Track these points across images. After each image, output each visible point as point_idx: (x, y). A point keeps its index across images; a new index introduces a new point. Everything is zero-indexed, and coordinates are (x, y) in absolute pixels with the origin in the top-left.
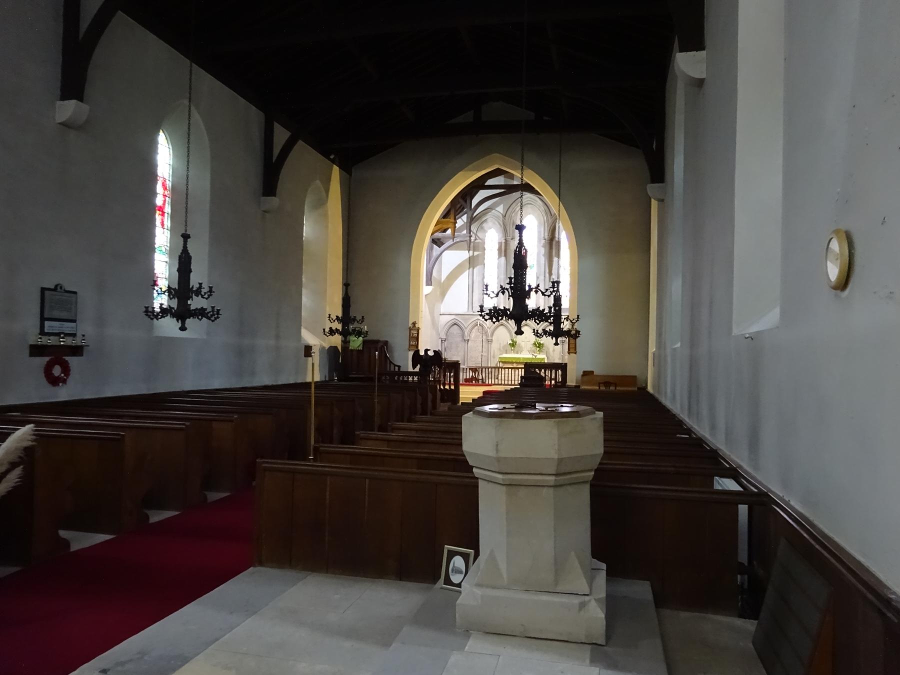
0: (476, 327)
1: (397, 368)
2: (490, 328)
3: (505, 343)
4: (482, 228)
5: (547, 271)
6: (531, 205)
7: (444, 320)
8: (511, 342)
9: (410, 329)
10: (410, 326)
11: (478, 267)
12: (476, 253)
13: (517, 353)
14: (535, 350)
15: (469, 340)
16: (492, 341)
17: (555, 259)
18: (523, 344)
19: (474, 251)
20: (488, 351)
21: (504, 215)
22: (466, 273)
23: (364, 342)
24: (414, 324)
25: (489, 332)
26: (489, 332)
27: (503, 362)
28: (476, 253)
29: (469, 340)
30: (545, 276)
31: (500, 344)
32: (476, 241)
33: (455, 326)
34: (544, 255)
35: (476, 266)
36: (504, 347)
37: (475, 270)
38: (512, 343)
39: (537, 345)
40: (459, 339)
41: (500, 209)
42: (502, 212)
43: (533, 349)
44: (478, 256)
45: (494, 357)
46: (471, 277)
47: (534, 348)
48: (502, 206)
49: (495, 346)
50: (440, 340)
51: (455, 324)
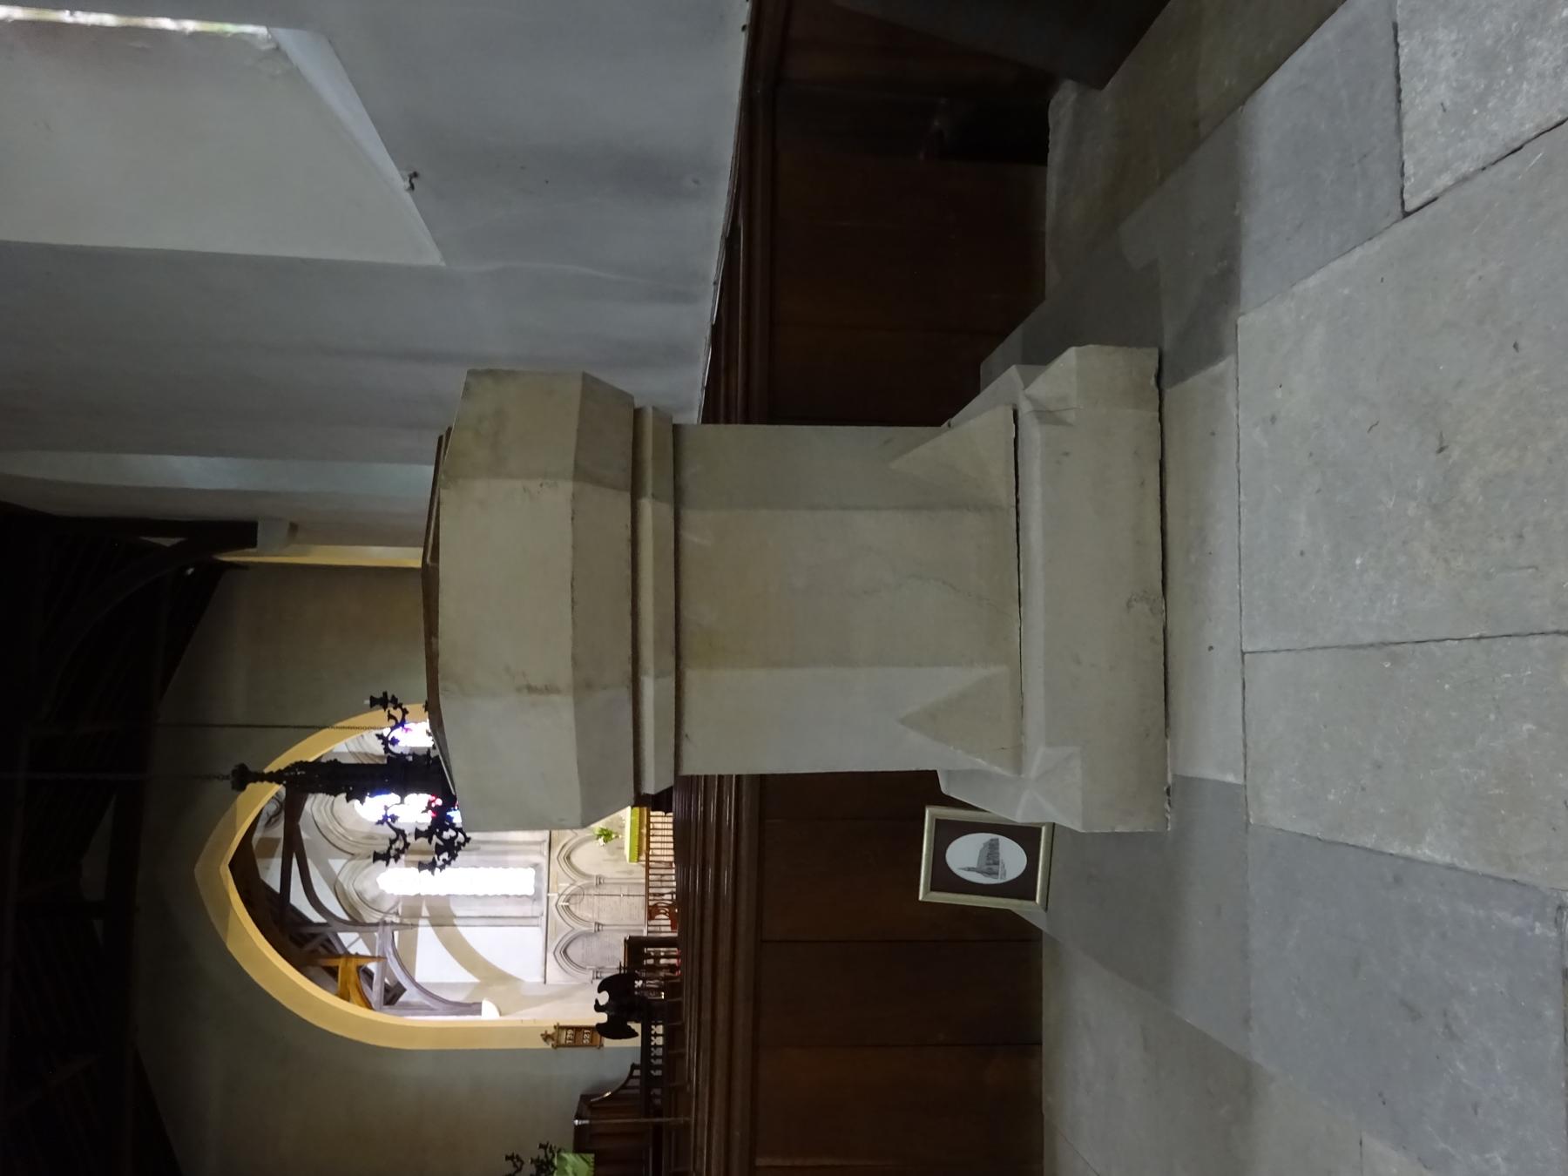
0: (572, 908)
1: (637, 1073)
3: (603, 850)
4: (374, 900)
7: (556, 974)
8: (601, 840)
9: (557, 1046)
10: (550, 1046)
12: (425, 912)
13: (623, 827)
15: (596, 923)
16: (599, 878)
19: (419, 916)
20: (618, 884)
21: (349, 856)
22: (460, 929)
23: (579, 1149)
24: (546, 1037)
25: (581, 882)
26: (581, 882)
27: (639, 854)
28: (425, 912)
31: (605, 860)
33: (569, 951)
35: (449, 908)
36: (612, 853)
37: (458, 913)
38: (602, 838)
40: (595, 943)
41: (337, 864)
42: (344, 861)
44: (429, 909)
45: (631, 872)
48: (332, 862)
49: (610, 871)
51: (565, 952)
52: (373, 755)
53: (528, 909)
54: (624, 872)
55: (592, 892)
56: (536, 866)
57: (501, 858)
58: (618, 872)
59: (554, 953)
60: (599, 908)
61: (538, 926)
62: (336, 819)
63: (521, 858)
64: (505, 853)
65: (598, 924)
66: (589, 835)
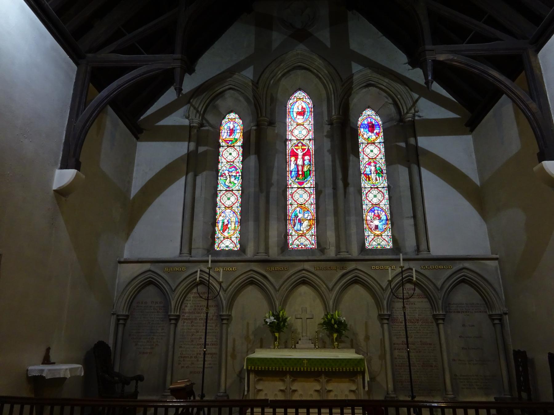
2: (225, 291)
5: (340, 176)
6: (303, 71)
11: (204, 173)
12: (201, 149)
14: (327, 340)
15: (179, 316)
16: (229, 318)
17: (352, 158)
18: (298, 325)
19: (198, 145)
22: (182, 180)
29: (179, 316)
30: (335, 188)
31: (248, 324)
32: (203, 128)
34: (332, 151)
35: (204, 171)
37: (200, 179)
39: (336, 326)
43: (320, 336)
45: (234, 356)
46: (189, 189)
47: (323, 334)
48: (251, 69)
50: (113, 319)
52: (350, 94)
53: (199, 243)
54: (234, 350)
55: (212, 311)
56: (243, 249)
57: (251, 215)
58: (234, 340)
59: (150, 271)
60: (195, 319)
61: (180, 253)
62: (288, 72)
63: (251, 235)
64: (257, 220)
65: (177, 319)
66: (277, 303)
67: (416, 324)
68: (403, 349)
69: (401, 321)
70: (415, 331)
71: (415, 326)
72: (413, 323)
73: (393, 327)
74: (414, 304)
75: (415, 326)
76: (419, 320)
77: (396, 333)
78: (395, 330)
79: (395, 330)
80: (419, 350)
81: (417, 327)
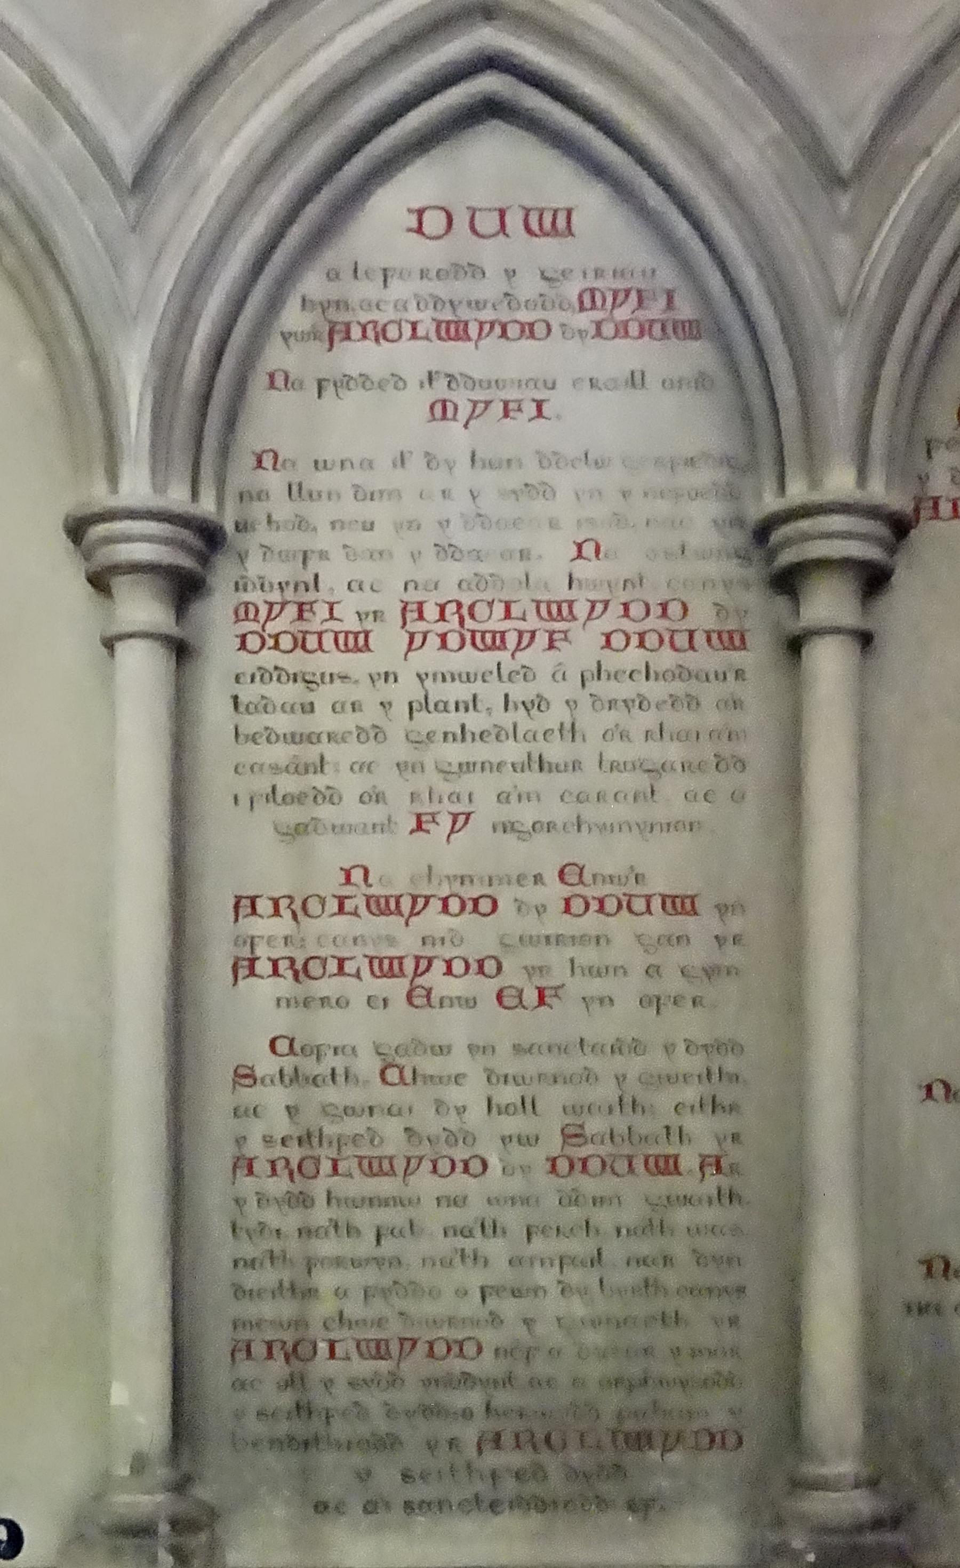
67: (535, 656)
68: (341, 962)
69: (352, 624)
70: (513, 751)
71: (519, 691)
72: (497, 642)
73: (248, 693)
74: (539, 405)
75: (519, 691)
76: (581, 610)
77: (276, 769)
78: (271, 736)
79: (271, 736)
80: (542, 970)
81: (539, 704)
